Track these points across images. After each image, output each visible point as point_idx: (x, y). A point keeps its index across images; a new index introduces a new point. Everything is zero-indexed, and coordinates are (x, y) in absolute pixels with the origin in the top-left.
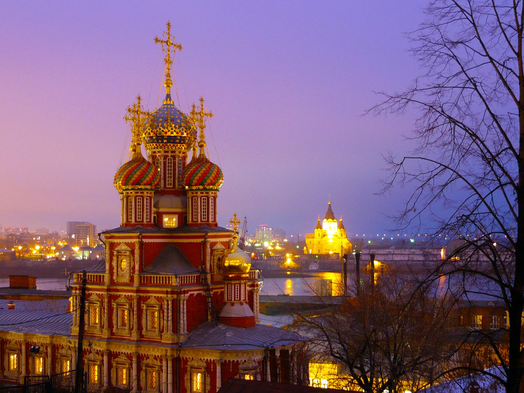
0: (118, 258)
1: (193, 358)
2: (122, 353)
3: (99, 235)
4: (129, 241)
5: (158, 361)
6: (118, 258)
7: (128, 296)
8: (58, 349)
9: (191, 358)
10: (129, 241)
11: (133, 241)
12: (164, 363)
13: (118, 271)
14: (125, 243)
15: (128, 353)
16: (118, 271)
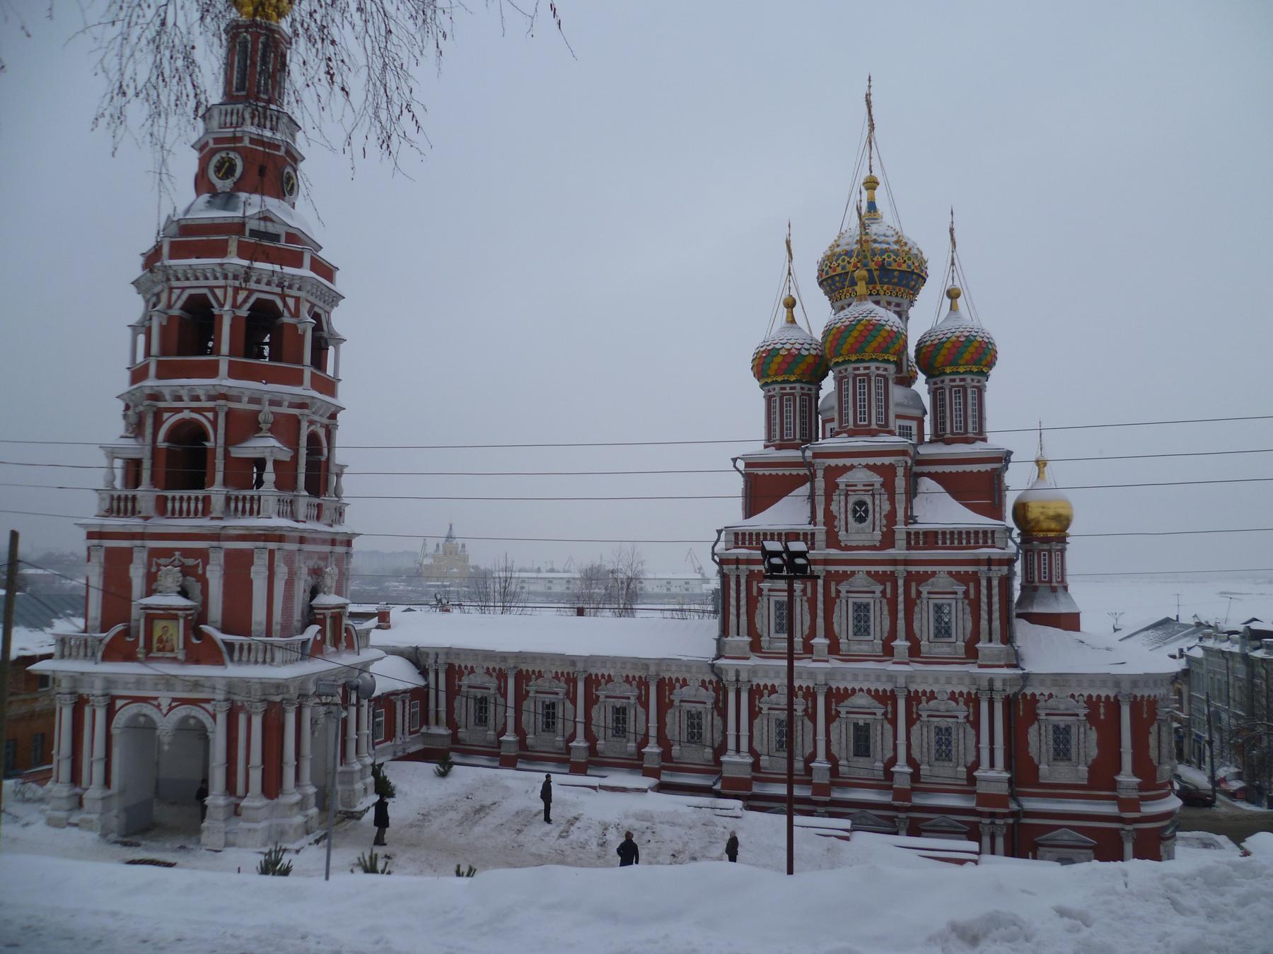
0: (847, 495)
1: (1051, 696)
2: (861, 690)
3: (735, 460)
4: (879, 461)
5: (961, 704)
6: (847, 495)
7: (877, 572)
8: (672, 688)
9: (1047, 693)
10: (879, 461)
11: (887, 460)
12: (984, 706)
13: (847, 524)
14: (868, 467)
15: (877, 691)
16: (847, 524)
